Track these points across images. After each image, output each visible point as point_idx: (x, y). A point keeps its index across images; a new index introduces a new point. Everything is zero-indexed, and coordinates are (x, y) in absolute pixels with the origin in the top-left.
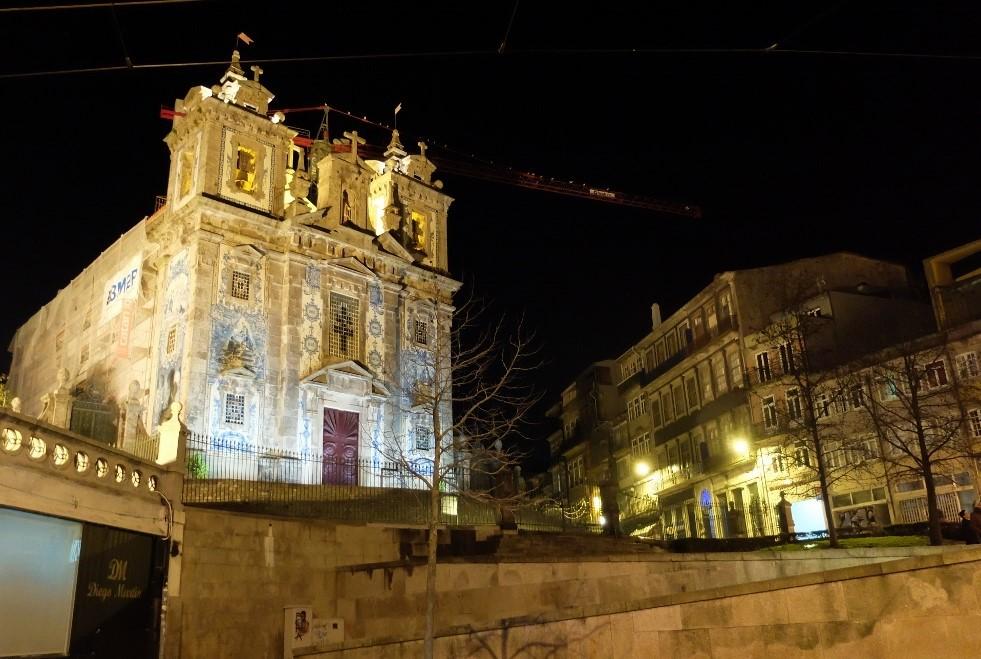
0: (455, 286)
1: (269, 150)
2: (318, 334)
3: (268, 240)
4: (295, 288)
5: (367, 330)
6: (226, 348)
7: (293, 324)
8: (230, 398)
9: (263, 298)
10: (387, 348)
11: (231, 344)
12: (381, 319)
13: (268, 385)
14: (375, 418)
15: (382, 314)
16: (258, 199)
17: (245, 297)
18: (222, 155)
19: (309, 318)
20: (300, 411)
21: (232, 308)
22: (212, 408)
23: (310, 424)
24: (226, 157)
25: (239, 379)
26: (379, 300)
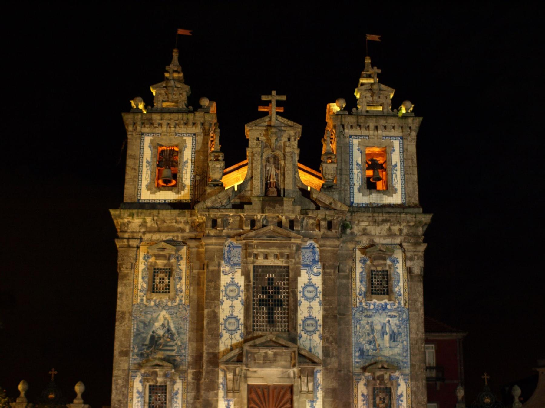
0: (427, 218)
1: (189, 141)
2: (239, 312)
3: (187, 230)
4: (213, 271)
5: (299, 296)
6: (147, 342)
7: (211, 308)
8: (153, 389)
9: (184, 288)
10: (325, 310)
11: (152, 337)
12: (318, 281)
13: (190, 371)
14: (311, 389)
15: (317, 274)
16: (178, 193)
17: (167, 290)
18: (141, 162)
19: (229, 297)
20: (221, 393)
21: (152, 303)
22: (135, 401)
23: (232, 403)
24: (145, 161)
25: (158, 370)
26: (314, 261)
